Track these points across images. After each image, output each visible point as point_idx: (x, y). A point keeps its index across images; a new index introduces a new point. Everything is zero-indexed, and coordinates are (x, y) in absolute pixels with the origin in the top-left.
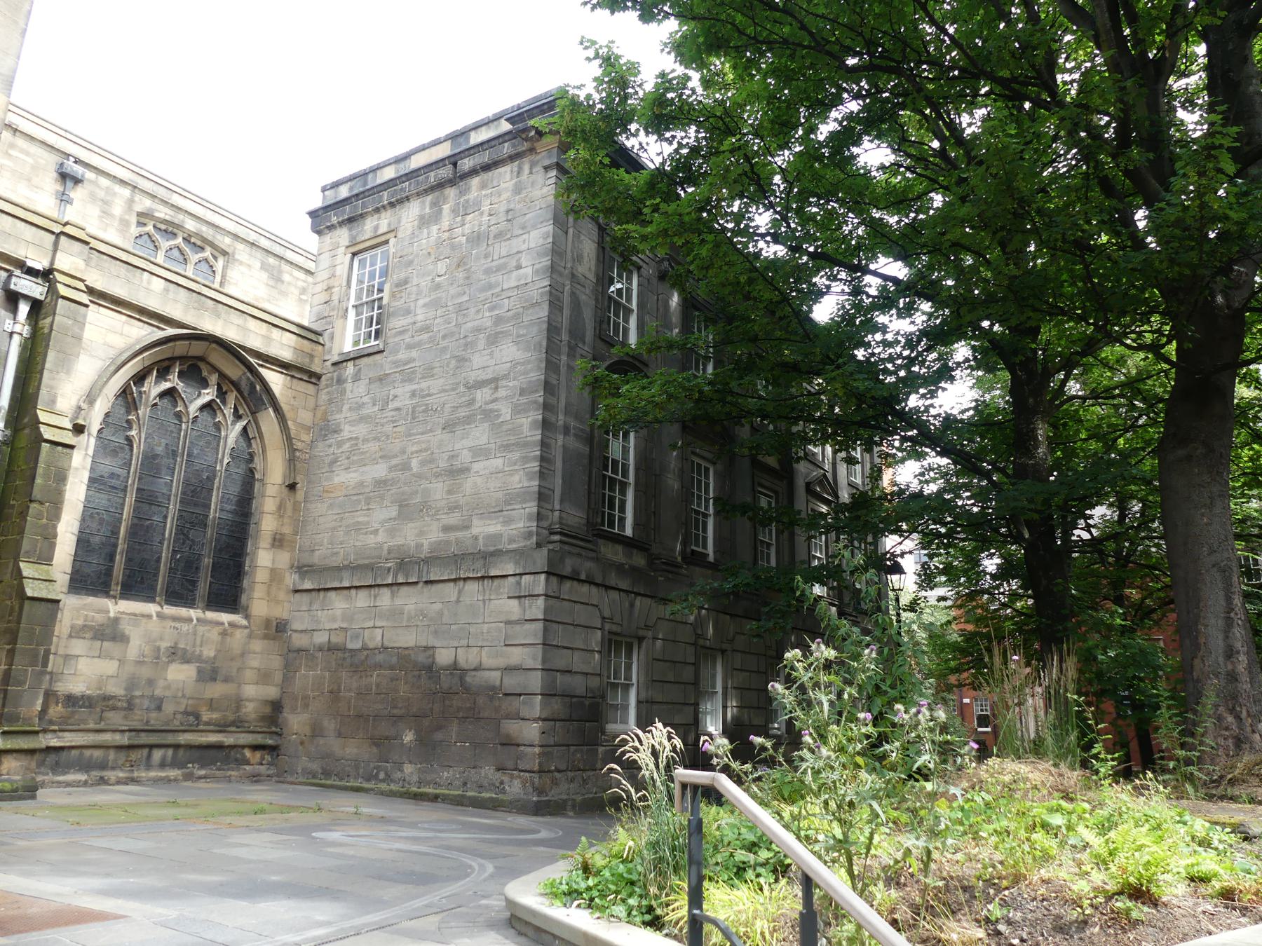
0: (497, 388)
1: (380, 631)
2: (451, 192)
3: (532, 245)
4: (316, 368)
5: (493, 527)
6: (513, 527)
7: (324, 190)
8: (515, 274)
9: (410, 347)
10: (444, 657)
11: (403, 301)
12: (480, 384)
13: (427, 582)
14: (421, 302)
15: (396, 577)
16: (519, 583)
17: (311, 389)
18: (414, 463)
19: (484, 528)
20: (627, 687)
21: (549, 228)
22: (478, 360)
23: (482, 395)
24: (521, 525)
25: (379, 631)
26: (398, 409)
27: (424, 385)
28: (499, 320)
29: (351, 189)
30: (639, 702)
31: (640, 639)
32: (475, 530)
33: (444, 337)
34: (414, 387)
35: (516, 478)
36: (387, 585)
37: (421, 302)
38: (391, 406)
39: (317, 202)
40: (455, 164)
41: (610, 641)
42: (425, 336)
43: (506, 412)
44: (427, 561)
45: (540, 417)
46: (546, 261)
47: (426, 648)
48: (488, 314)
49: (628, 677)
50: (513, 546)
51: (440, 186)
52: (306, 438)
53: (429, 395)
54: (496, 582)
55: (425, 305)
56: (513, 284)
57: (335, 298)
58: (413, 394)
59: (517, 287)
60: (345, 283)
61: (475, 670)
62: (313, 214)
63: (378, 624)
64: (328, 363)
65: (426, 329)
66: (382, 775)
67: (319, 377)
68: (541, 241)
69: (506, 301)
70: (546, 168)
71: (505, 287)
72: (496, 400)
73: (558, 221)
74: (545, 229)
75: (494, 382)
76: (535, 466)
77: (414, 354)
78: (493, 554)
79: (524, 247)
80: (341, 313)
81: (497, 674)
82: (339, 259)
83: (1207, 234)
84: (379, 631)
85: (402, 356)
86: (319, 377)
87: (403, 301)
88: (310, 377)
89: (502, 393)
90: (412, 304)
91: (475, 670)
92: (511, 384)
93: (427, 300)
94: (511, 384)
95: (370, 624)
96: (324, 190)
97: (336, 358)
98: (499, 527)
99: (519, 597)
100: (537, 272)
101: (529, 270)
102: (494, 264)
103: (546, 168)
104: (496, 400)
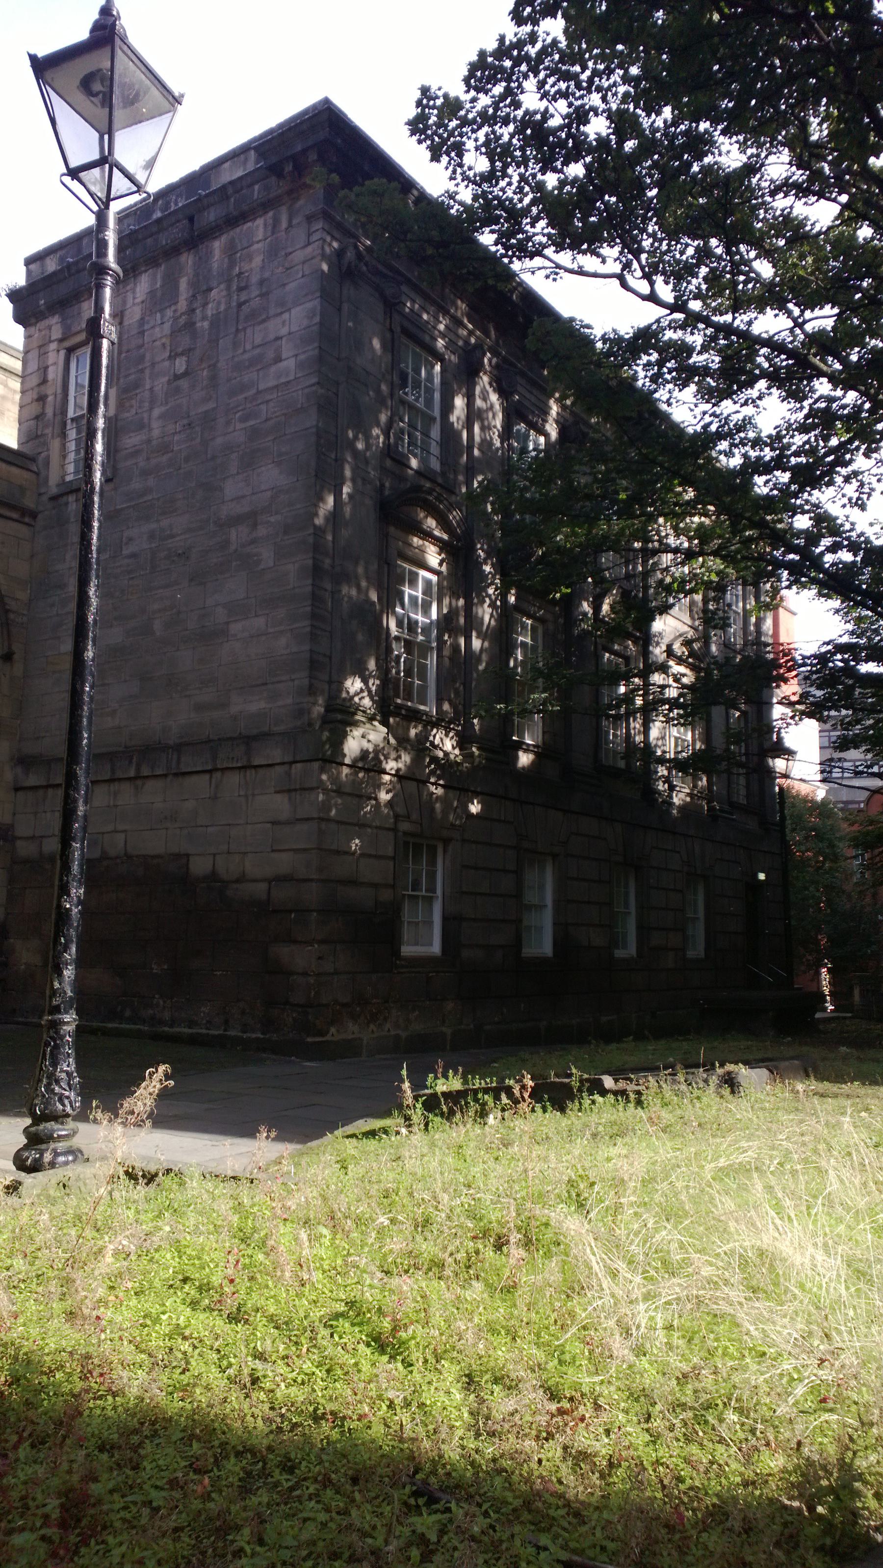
0: (255, 525)
1: (123, 836)
2: (188, 260)
3: (294, 328)
4: (29, 502)
5: (256, 705)
6: (280, 703)
7: (28, 262)
8: (273, 369)
9: (145, 473)
10: (199, 866)
11: (133, 411)
12: (236, 520)
13: (176, 775)
14: (156, 412)
15: (138, 769)
16: (288, 774)
17: (24, 531)
18: (157, 625)
19: (252, 705)
20: (429, 900)
21: (314, 304)
22: (231, 489)
23: (237, 535)
24: (289, 701)
25: (122, 836)
26: (133, 556)
27: (165, 523)
28: (254, 434)
29: (62, 259)
30: (445, 919)
31: (446, 842)
32: (234, 709)
33: (187, 460)
34: (154, 526)
35: (283, 641)
36: (129, 779)
37: (156, 412)
38: (126, 552)
39: (20, 279)
40: (191, 219)
41: (406, 844)
42: (164, 459)
43: (267, 555)
44: (179, 748)
45: (310, 562)
46: (312, 350)
47: (177, 856)
48: (239, 426)
49: (432, 889)
50: (282, 728)
51: (173, 252)
52: (23, 595)
53: (172, 536)
54: (261, 771)
55: (161, 417)
56: (272, 383)
57: (49, 411)
58: (152, 536)
59: (277, 386)
60: (59, 391)
61: (237, 881)
62: (14, 296)
63: (120, 827)
64: (45, 498)
65: (165, 448)
66: (128, 1013)
67: (34, 515)
68: (306, 322)
69: (263, 407)
70: (310, 219)
71: (262, 387)
72: (253, 542)
73: (325, 295)
74: (309, 305)
75: (251, 518)
76: (304, 625)
77: (151, 482)
78: (255, 738)
79: (284, 331)
80: (57, 430)
81: (264, 886)
82: (52, 357)
83: (756, 876)
84: (122, 836)
85: (136, 485)
86: (34, 515)
87: (133, 411)
88: (23, 515)
89: (262, 531)
90: (146, 415)
91: (237, 881)
92: (272, 519)
93: (163, 409)
94: (272, 519)
95: (110, 828)
96: (28, 262)
97: (54, 491)
98: (263, 705)
99: (289, 791)
100: (300, 366)
101: (290, 364)
102: (246, 356)
103: (310, 219)
104: (253, 542)
